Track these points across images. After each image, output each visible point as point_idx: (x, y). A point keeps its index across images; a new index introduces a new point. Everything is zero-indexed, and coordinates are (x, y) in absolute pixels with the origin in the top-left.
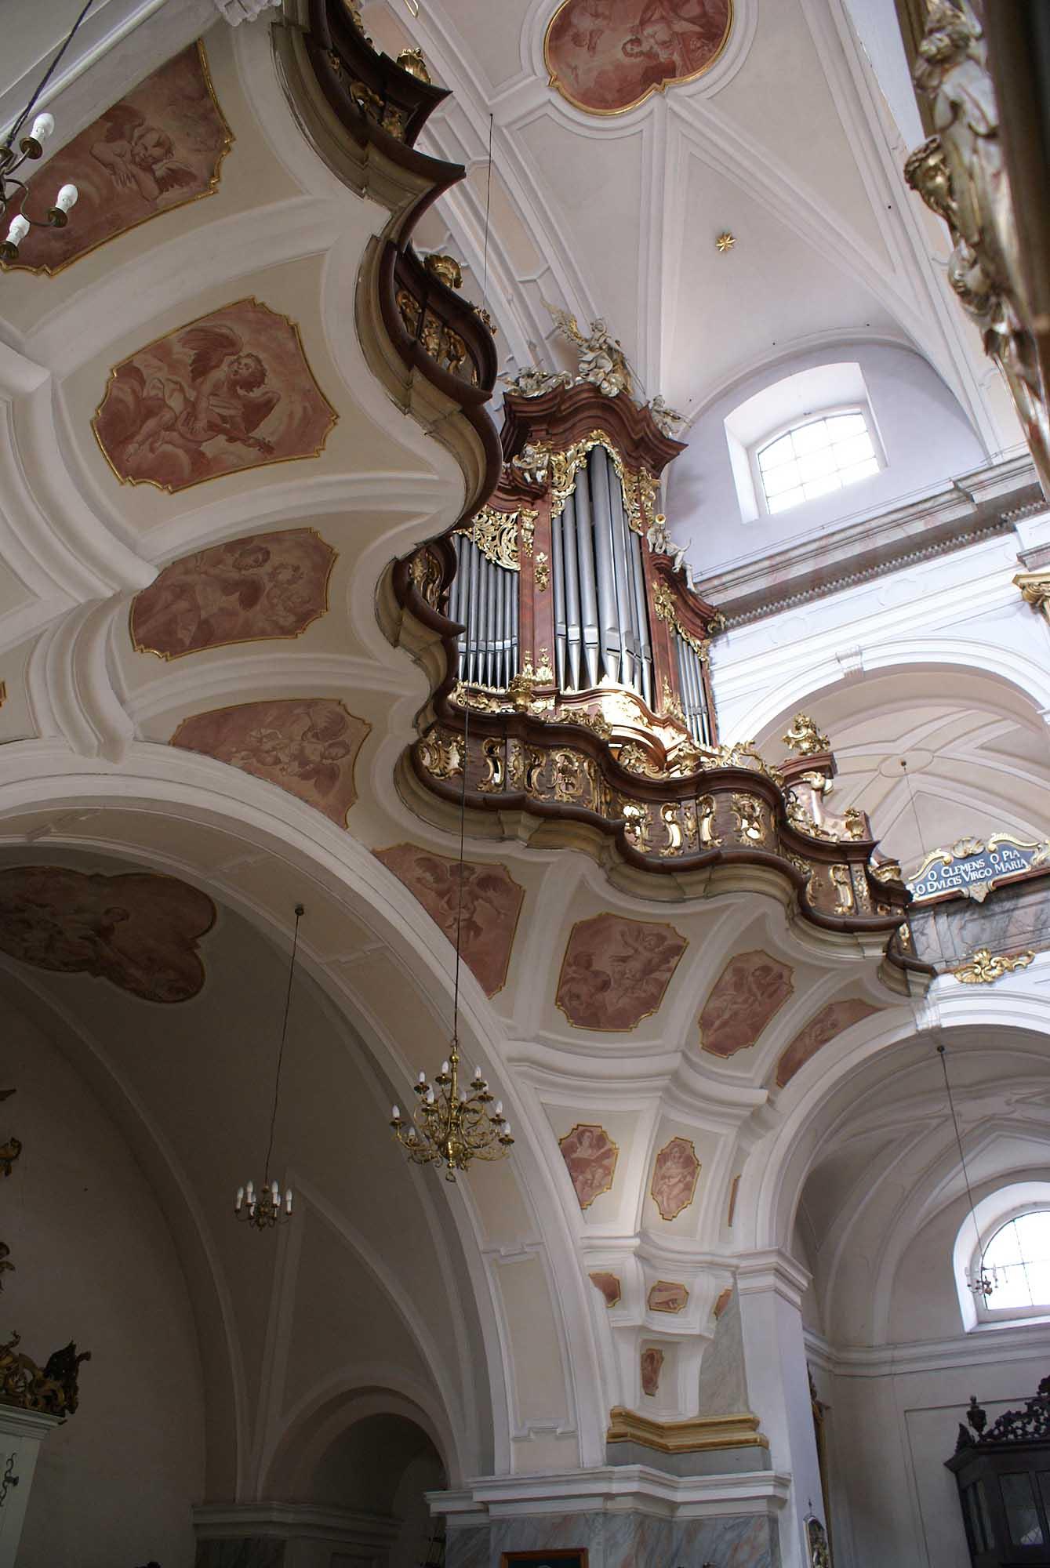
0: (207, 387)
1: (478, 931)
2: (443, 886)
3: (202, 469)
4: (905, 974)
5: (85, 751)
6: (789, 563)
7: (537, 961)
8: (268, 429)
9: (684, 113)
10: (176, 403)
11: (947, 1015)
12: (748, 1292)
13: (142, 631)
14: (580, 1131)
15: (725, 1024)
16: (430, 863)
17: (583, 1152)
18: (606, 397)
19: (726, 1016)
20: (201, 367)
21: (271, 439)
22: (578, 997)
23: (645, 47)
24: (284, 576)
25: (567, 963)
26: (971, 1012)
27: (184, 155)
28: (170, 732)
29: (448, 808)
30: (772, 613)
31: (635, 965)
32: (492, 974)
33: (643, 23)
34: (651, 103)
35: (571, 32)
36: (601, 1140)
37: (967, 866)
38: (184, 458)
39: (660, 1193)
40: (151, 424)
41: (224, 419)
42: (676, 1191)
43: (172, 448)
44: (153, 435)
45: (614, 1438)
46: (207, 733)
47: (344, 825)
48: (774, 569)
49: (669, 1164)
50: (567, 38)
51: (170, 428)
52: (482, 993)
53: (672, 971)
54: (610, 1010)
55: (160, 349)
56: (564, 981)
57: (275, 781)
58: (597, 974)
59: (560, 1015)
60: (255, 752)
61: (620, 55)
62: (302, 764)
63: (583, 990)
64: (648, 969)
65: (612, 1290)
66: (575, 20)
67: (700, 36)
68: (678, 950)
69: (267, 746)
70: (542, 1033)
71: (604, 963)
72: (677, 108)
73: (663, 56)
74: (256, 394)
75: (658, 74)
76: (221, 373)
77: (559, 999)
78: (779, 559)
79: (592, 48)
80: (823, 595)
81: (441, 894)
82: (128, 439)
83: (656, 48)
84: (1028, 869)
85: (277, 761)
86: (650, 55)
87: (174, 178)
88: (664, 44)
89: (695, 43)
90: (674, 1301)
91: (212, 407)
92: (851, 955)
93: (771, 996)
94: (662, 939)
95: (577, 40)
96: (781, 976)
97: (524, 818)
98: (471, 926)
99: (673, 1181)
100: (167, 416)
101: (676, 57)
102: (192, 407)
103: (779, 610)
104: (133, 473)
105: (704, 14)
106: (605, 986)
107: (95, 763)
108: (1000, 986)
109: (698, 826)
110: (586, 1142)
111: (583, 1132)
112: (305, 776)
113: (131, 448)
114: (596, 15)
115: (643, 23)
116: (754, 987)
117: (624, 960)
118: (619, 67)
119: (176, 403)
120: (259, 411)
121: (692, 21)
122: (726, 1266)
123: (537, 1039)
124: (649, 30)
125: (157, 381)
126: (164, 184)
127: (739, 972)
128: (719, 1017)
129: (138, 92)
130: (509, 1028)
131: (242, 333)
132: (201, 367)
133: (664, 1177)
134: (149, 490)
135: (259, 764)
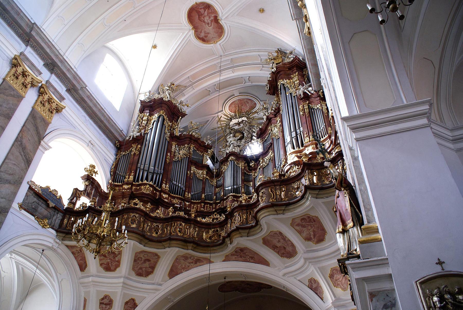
1: (253, 257)
2: (239, 256)
3: (119, 262)
5: (155, 293)
9: (226, 16)
10: (109, 261)
15: (314, 236)
16: (232, 255)
18: (276, 71)
19: (312, 233)
22: (284, 253)
23: (210, 22)
25: (274, 250)
29: (221, 246)
31: (282, 240)
32: (265, 262)
33: (204, 22)
34: (222, 22)
35: (204, 38)
39: (338, 285)
40: (110, 264)
42: (343, 281)
44: (111, 265)
46: (173, 273)
47: (213, 262)
49: (335, 276)
50: (205, 39)
56: (278, 253)
57: (193, 268)
58: (280, 247)
60: (183, 268)
61: (211, 27)
62: (192, 263)
63: (283, 251)
66: (201, 37)
67: (209, 9)
68: (281, 233)
69: (184, 266)
70: (286, 265)
71: (279, 245)
72: (224, 17)
73: (212, 18)
75: (216, 20)
76: (107, 255)
77: (281, 256)
79: (208, 33)
81: (241, 257)
82: (110, 268)
83: (210, 19)
85: (189, 266)
86: (212, 21)
87: (81, 251)
88: (210, 17)
89: (210, 11)
91: (111, 257)
92: (308, 203)
93: (314, 221)
95: (206, 37)
99: (340, 280)
100: (110, 262)
101: (213, 15)
104: (114, 270)
105: (204, 8)
106: (285, 248)
107: (158, 293)
109: (281, 193)
112: (196, 263)
114: (201, 32)
115: (204, 22)
117: (279, 241)
118: (213, 28)
119: (109, 261)
121: (205, 11)
124: (206, 21)
125: (105, 261)
126: (81, 252)
127: (298, 225)
128: (310, 235)
129: (71, 251)
130: (279, 269)
133: (336, 280)
134: (118, 269)
135: (187, 269)
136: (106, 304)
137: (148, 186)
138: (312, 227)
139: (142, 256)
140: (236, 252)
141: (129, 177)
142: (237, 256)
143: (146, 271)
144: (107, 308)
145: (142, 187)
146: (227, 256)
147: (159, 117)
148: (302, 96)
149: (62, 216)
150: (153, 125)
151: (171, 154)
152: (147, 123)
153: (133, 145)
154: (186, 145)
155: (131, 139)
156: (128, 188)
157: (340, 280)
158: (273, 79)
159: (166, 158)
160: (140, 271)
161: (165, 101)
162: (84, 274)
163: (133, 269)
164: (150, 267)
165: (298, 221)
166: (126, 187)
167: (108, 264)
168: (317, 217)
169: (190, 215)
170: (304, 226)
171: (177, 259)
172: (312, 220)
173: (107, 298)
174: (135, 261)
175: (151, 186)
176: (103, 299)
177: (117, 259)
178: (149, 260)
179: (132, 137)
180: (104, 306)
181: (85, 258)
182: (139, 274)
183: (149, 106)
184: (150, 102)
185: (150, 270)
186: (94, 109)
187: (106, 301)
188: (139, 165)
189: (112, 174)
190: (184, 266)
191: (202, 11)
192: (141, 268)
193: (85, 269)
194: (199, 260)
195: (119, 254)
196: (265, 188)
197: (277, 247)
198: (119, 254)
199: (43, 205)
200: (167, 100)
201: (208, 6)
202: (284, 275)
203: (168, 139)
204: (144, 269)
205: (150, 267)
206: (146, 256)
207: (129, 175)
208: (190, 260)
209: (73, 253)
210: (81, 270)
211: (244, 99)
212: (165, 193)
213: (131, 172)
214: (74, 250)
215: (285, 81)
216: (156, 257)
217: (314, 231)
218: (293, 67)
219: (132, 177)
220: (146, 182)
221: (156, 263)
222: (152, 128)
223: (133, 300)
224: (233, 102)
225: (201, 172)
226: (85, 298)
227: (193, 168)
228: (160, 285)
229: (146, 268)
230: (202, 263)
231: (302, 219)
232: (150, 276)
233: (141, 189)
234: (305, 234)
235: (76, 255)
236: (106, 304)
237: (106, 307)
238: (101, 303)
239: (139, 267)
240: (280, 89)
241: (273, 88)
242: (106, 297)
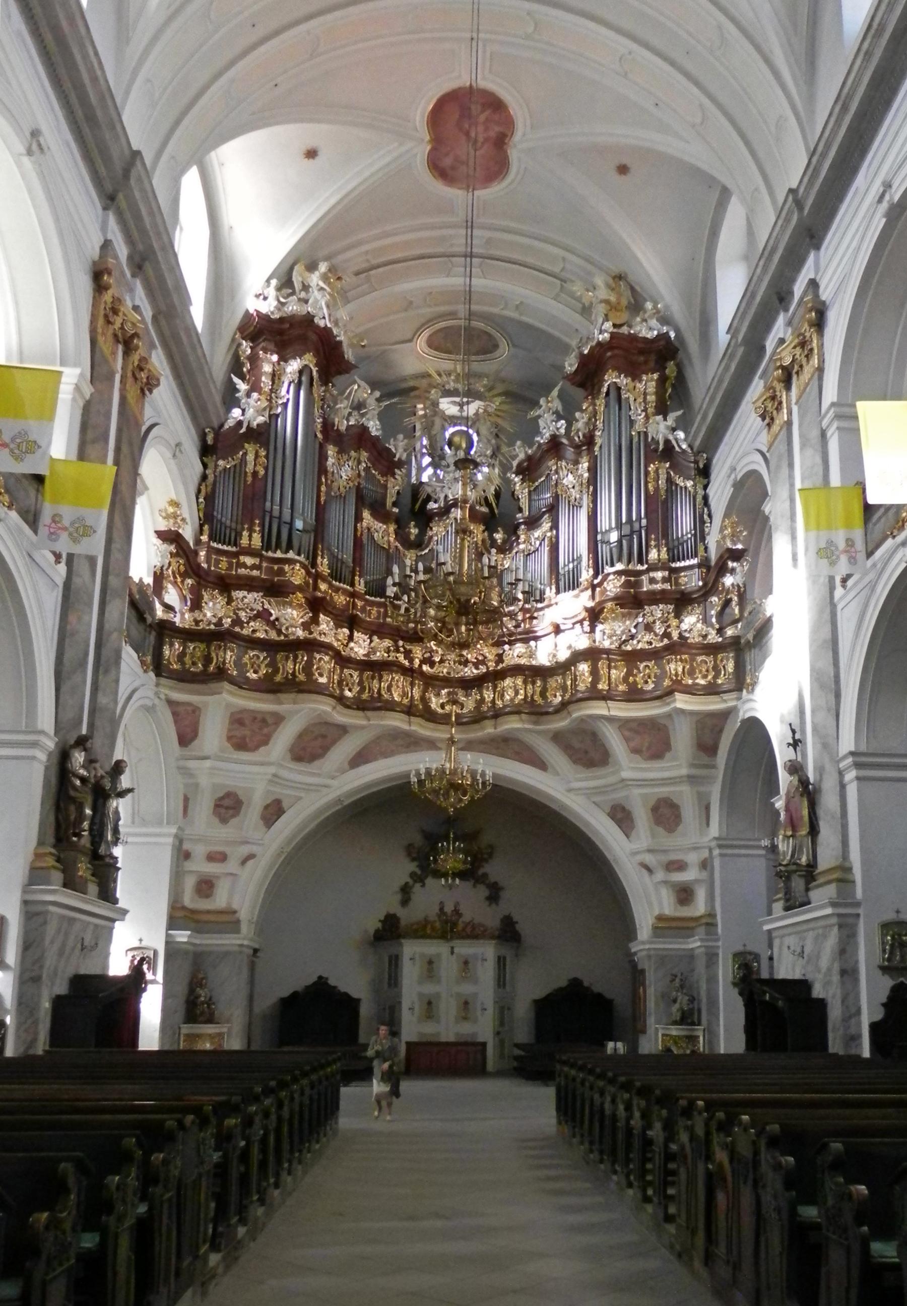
137: (298, 567)
141: (250, 536)
145: (286, 567)
147: (301, 372)
150: (288, 392)
151: (326, 480)
152: (273, 383)
153: (246, 445)
154: (353, 453)
155: (243, 430)
156: (253, 567)
161: (318, 327)
166: (249, 561)
169: (411, 661)
175: (303, 566)
179: (245, 425)
184: (281, 320)
186: (192, 358)
188: (268, 504)
189: (201, 515)
191: (475, 109)
200: (322, 323)
201: (495, 105)
203: (319, 435)
207: (251, 531)
212: (324, 580)
213: (252, 524)
219: (257, 541)
220: (291, 555)
222: (288, 400)
225: (379, 526)
233: (281, 572)
241: (588, 375)
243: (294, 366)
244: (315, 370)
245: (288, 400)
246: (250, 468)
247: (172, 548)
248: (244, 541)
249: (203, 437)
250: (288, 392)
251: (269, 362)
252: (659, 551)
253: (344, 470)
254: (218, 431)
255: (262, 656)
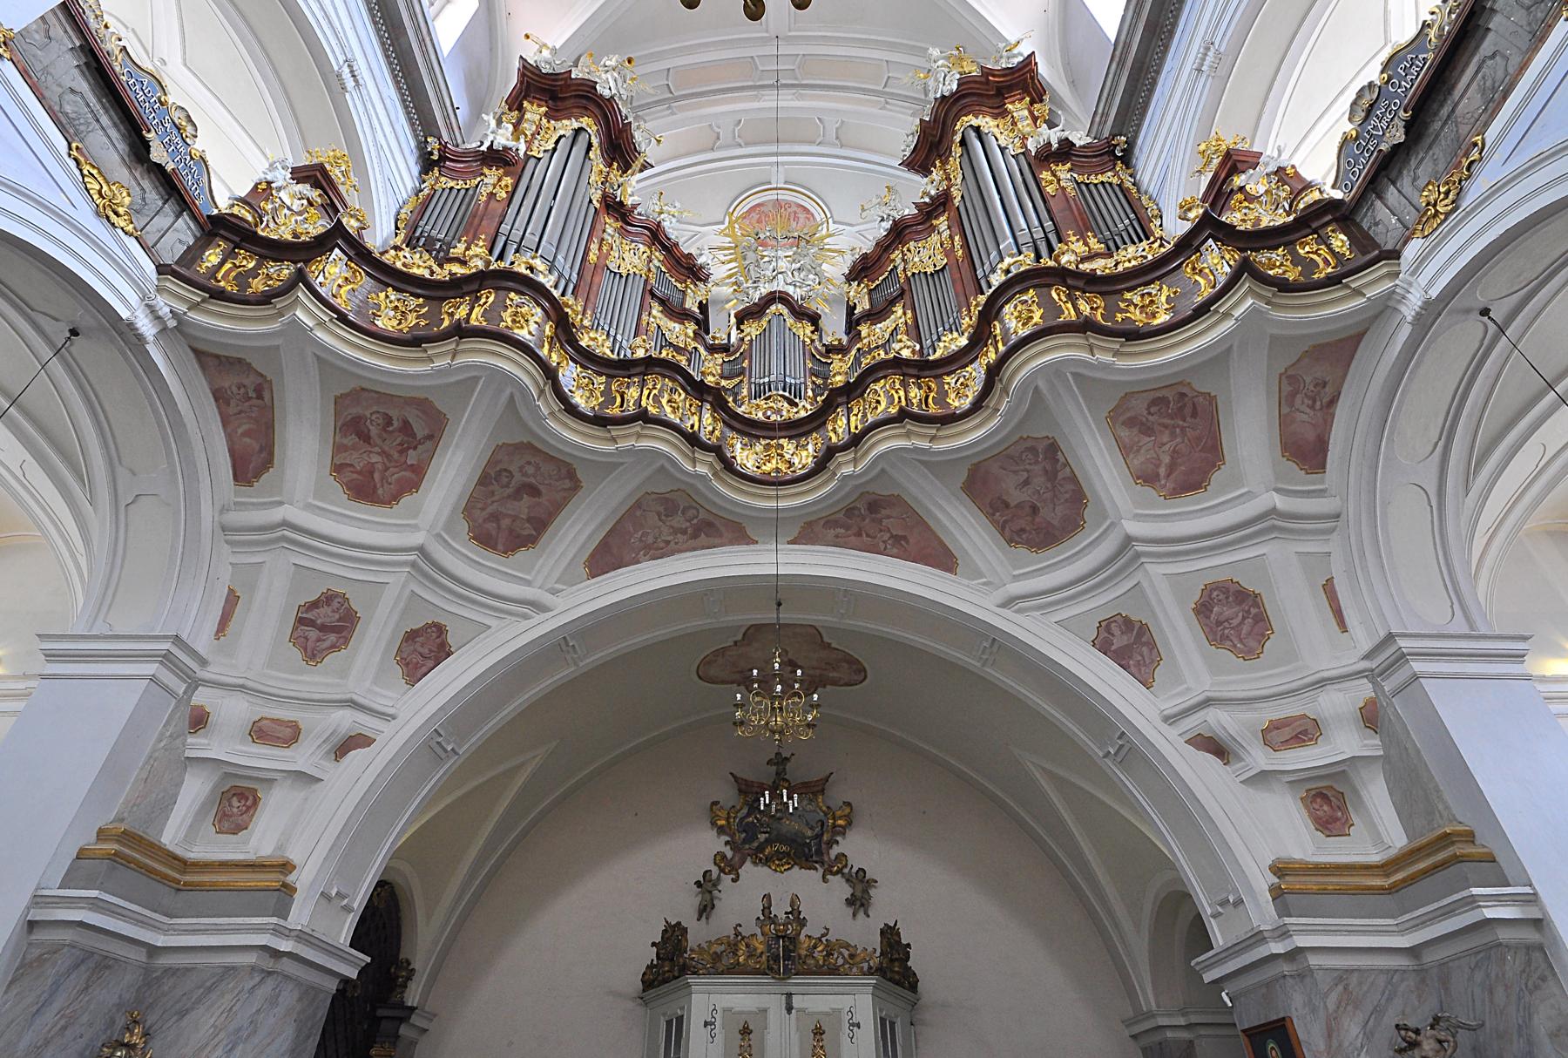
0: (379, 441)
1: (904, 538)
2: (855, 529)
4: (1347, 286)
6: (1127, 45)
7: (965, 527)
8: (420, 432)
10: (375, 459)
11: (1431, 283)
12: (1396, 693)
13: (500, 547)
14: (1105, 626)
15: (1171, 468)
16: (830, 523)
17: (1119, 641)
18: (953, 94)
19: (1166, 459)
20: (366, 438)
21: (426, 432)
22: (1023, 530)
24: (530, 470)
26: (1452, 259)
27: (250, 381)
28: (584, 572)
30: (1151, 91)
31: (1039, 481)
32: (942, 558)
36: (1128, 623)
37: (1374, 121)
38: (407, 474)
40: (377, 476)
41: (401, 444)
42: (1245, 629)
43: (395, 476)
45: (1277, 894)
46: (604, 559)
48: (1121, 63)
51: (387, 469)
52: (948, 575)
53: (1067, 464)
54: (1055, 522)
55: (338, 449)
56: (1002, 529)
58: (1019, 506)
59: (1022, 551)
62: (684, 532)
63: (1022, 523)
64: (1051, 475)
65: (1217, 747)
68: (1053, 449)
69: (650, 540)
71: (1016, 496)
74: (396, 424)
76: (374, 431)
77: (1009, 541)
78: (1118, 53)
80: (1171, 33)
81: (859, 534)
84: (1430, 56)
85: (668, 542)
87: (259, 392)
90: (1305, 732)
93: (1194, 414)
94: (1033, 450)
96: (1183, 395)
97: (841, 457)
98: (897, 539)
100: (380, 466)
102: (383, 453)
103: (1154, 82)
104: (394, 499)
106: (1035, 510)
108: (1466, 203)
110: (1117, 632)
111: (1108, 626)
112: (695, 536)
113: (380, 491)
116: (1167, 421)
117: (1026, 483)
119: (375, 459)
120: (406, 427)
122: (1358, 674)
123: (1016, 578)
125: (358, 459)
126: (260, 397)
127: (1131, 423)
128: (1158, 466)
129: (210, 383)
131: (355, 411)
132: (366, 438)
135: (659, 550)
136: (323, 628)
138: (1173, 436)
139: (514, 468)
140: (850, 511)
142: (848, 528)
143: (511, 531)
144: (327, 644)
146: (810, 524)
147: (578, 131)
148: (1055, 146)
149: (197, 239)
153: (486, 171)
157: (1235, 622)
158: (935, 120)
159: (586, 253)
160: (491, 526)
162: (249, 495)
163: (468, 511)
164: (529, 520)
165: (1139, 406)
167: (370, 471)
168: (1211, 399)
170: (1147, 430)
171: (638, 505)
172: (1188, 410)
173: (335, 604)
174: (484, 480)
176: (314, 605)
177: (412, 457)
178: (534, 491)
180: (313, 634)
181: (270, 427)
182: (485, 540)
183: (548, 90)
185: (528, 530)
187: (325, 615)
188: (505, 228)
190: (650, 540)
192: (495, 517)
193: (257, 476)
194: (710, 525)
195: (430, 437)
196: (1034, 287)
197: (1007, 506)
198: (430, 437)
199: (114, 133)
200: (607, 93)
202: (1007, 603)
204: (505, 522)
205: (529, 520)
206: (530, 470)
208: (678, 521)
209: (219, 396)
210: (236, 478)
211: (789, 204)
214: (228, 382)
215: (987, 123)
216: (567, 484)
217: (1175, 454)
218: (1010, 88)
221: (557, 508)
222: (555, 149)
223: (440, 629)
224: (758, 205)
226: (231, 591)
227: (656, 310)
228: (554, 592)
229: (515, 518)
230: (717, 541)
231: (1154, 402)
232: (522, 555)
234: (1137, 462)
235: (232, 410)
236: (323, 628)
237: (319, 640)
238: (300, 621)
239: (490, 509)
240: (963, 143)
242: (328, 598)
243: (567, 126)
244: (595, 141)
245: (555, 149)
246: (484, 191)
247: (315, 194)
248: (459, 249)
249: (422, 146)
250: (557, 142)
251: (534, 112)
252: (1086, 244)
253: (632, 257)
254: (443, 148)
255: (413, 302)
